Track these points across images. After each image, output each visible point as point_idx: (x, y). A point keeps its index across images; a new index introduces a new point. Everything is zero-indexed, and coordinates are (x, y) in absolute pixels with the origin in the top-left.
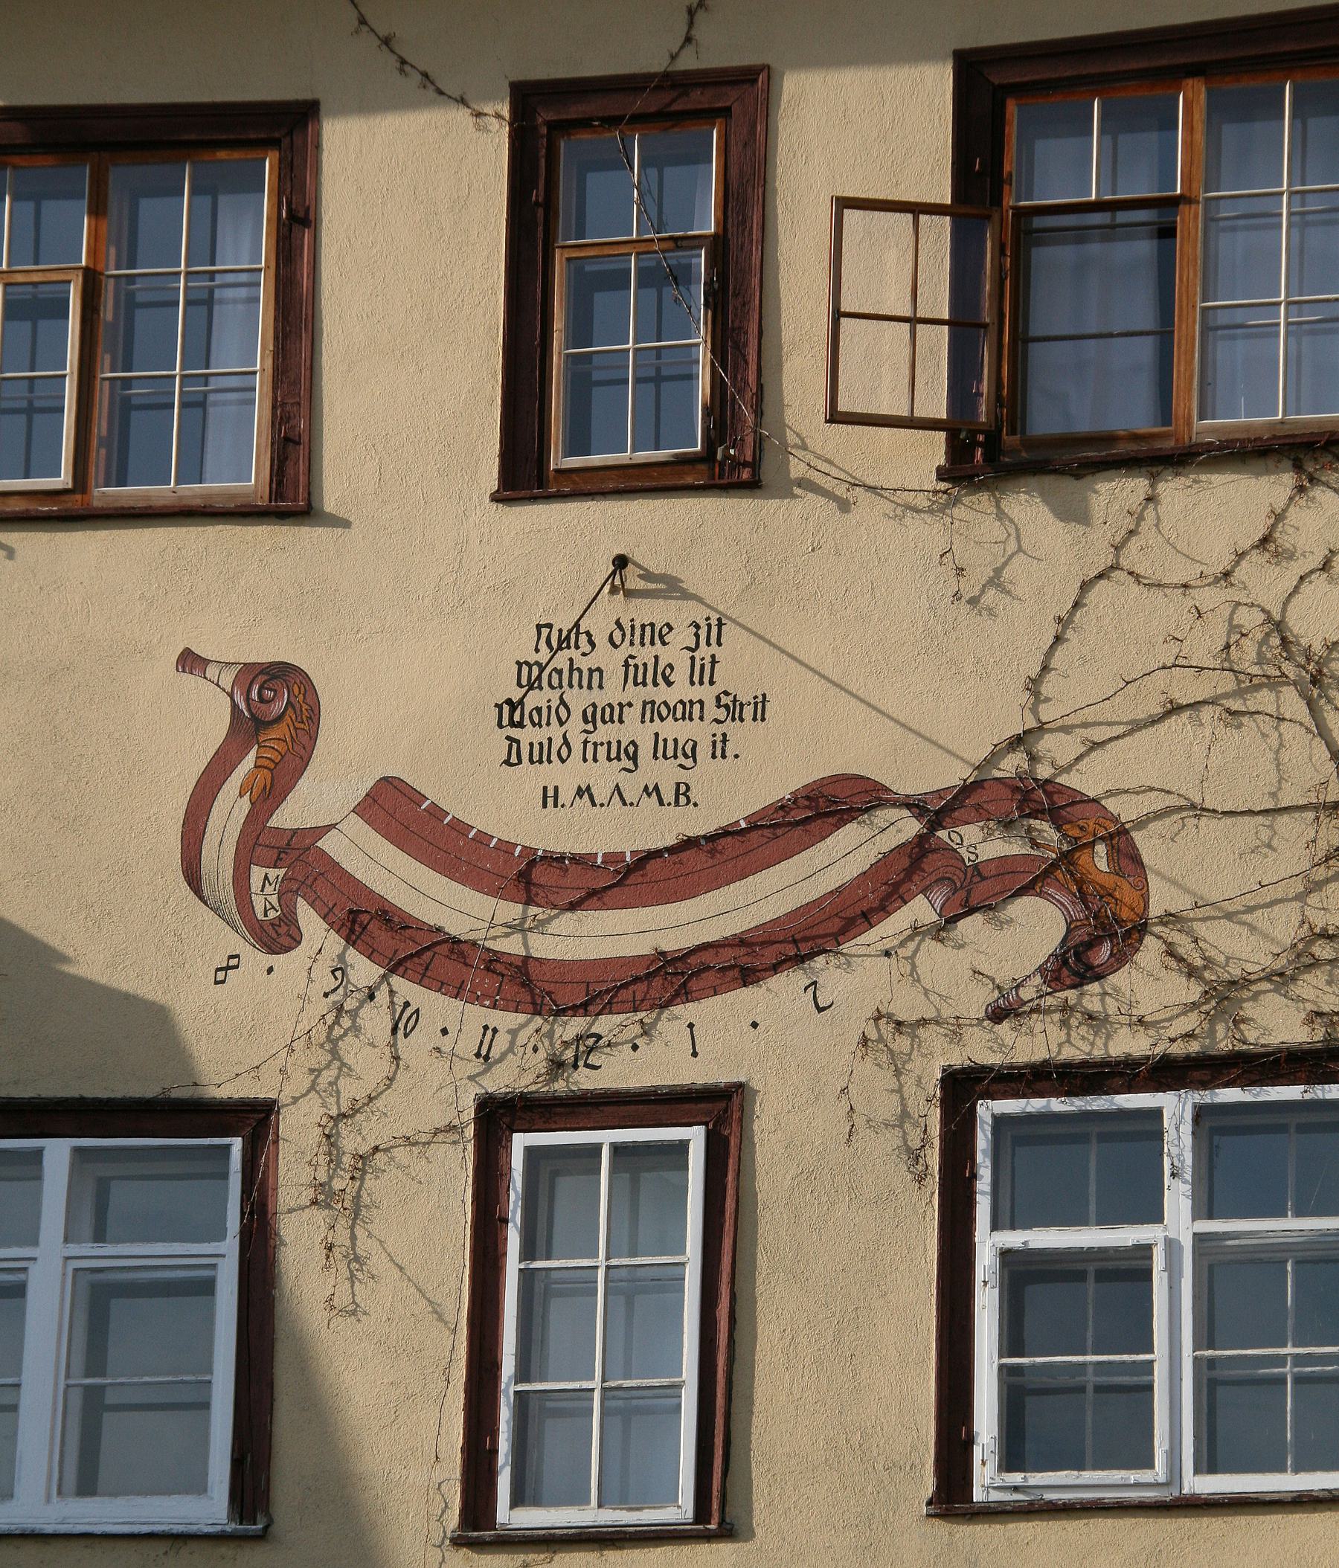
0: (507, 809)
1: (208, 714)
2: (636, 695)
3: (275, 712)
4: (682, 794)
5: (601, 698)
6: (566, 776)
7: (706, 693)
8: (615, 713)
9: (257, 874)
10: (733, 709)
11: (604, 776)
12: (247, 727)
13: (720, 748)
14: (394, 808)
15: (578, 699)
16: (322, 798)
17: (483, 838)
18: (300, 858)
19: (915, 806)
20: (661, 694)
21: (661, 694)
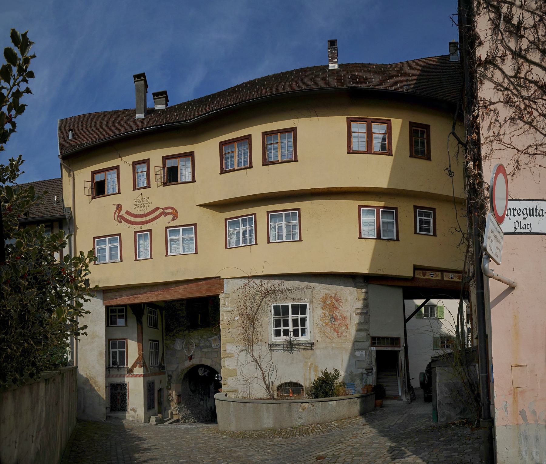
1: (115, 208)
3: (119, 207)
12: (117, 208)
14: (127, 213)
16: (123, 213)
18: (121, 217)
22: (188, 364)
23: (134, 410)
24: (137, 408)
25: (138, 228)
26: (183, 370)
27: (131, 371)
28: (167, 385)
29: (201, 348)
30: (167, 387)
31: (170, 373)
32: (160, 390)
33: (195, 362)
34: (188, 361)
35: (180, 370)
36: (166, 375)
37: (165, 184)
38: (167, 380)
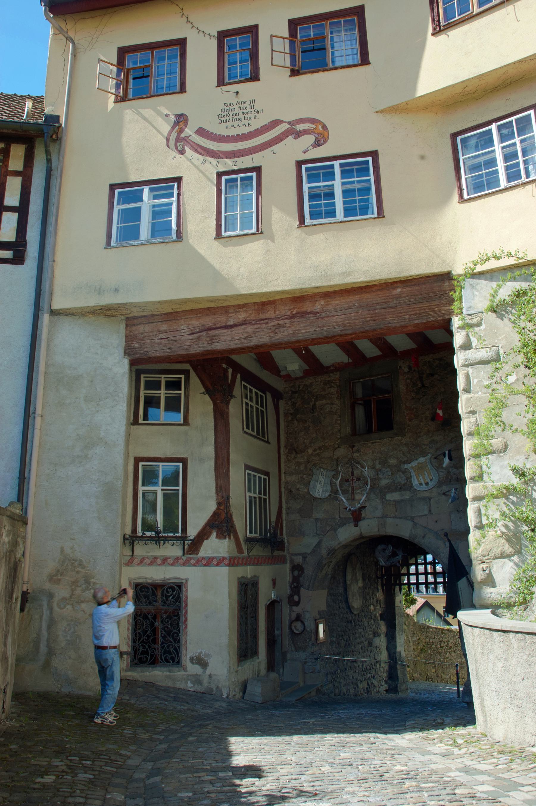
0: (220, 130)
2: (241, 111)
4: (249, 125)
5: (235, 113)
6: (229, 124)
7: (253, 110)
8: (237, 114)
9: (178, 144)
10: (257, 112)
11: (236, 123)
12: (177, 123)
13: (255, 118)
14: (201, 132)
15: (231, 113)
16: (189, 131)
17: (216, 134)
18: (186, 140)
19: (289, 123)
20: (245, 111)
21: (245, 111)
22: (347, 534)
23: (200, 661)
24: (206, 655)
25: (229, 164)
26: (332, 552)
27: (195, 545)
28: (288, 591)
29: (382, 492)
30: (291, 597)
31: (299, 560)
32: (272, 606)
33: (369, 527)
34: (352, 524)
35: (324, 552)
36: (288, 566)
37: (295, 73)
38: (288, 578)
